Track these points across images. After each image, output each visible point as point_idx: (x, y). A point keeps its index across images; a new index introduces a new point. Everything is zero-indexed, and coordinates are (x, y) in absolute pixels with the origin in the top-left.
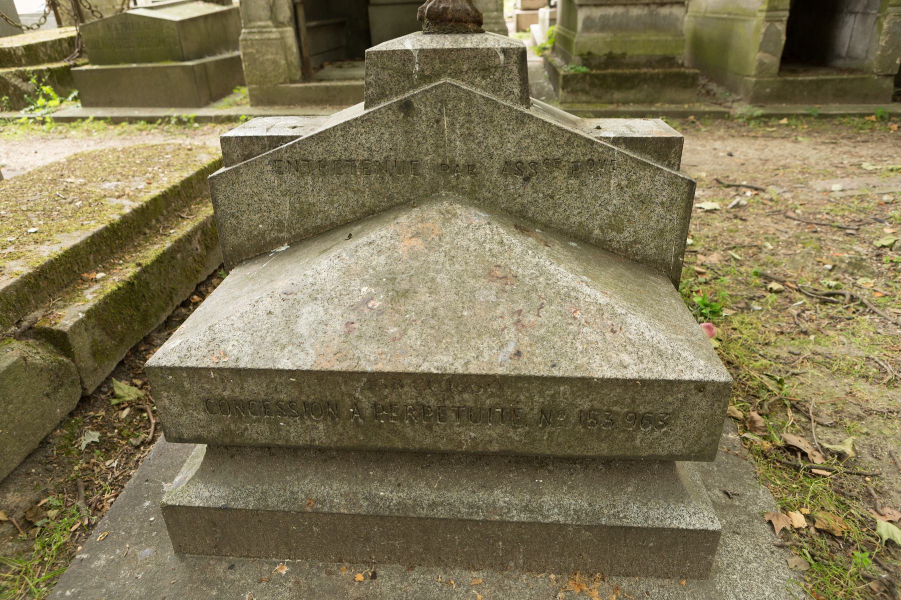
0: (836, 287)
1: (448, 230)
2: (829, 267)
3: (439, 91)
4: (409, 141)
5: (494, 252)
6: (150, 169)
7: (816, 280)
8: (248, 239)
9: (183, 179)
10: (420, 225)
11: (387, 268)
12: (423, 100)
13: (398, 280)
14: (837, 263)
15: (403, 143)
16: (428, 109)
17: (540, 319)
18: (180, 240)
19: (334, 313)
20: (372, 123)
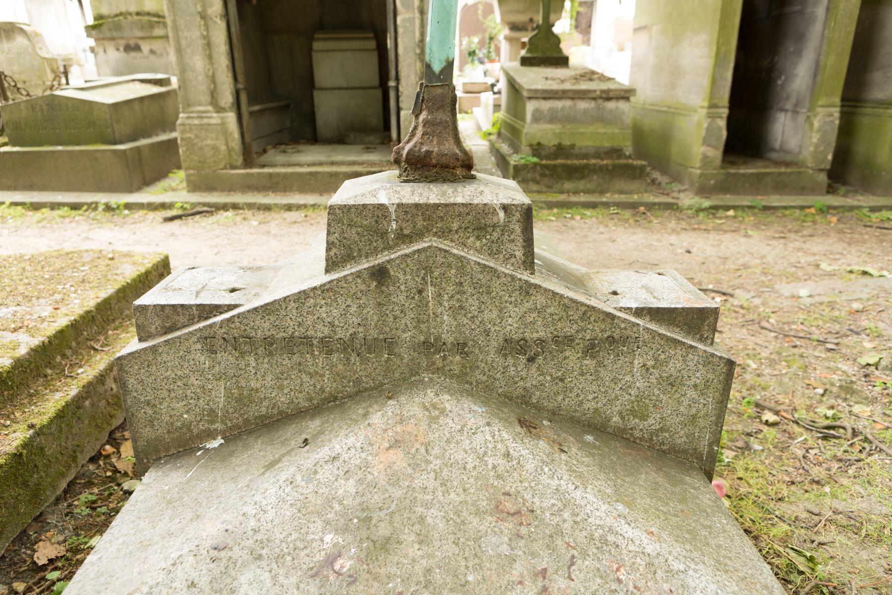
0: (834, 418)
1: (437, 435)
2: (821, 391)
3: (423, 257)
4: (383, 315)
5: (500, 469)
6: (60, 287)
7: (809, 408)
8: (169, 432)
9: (99, 300)
10: (399, 428)
11: (359, 499)
12: (402, 266)
13: (374, 521)
14: (828, 386)
15: (375, 318)
16: (409, 277)
17: (572, 584)
18: (90, 384)
19: (285, 582)
20: (336, 293)
